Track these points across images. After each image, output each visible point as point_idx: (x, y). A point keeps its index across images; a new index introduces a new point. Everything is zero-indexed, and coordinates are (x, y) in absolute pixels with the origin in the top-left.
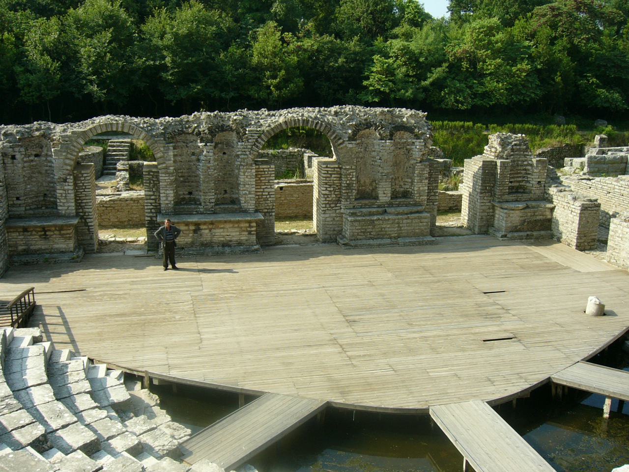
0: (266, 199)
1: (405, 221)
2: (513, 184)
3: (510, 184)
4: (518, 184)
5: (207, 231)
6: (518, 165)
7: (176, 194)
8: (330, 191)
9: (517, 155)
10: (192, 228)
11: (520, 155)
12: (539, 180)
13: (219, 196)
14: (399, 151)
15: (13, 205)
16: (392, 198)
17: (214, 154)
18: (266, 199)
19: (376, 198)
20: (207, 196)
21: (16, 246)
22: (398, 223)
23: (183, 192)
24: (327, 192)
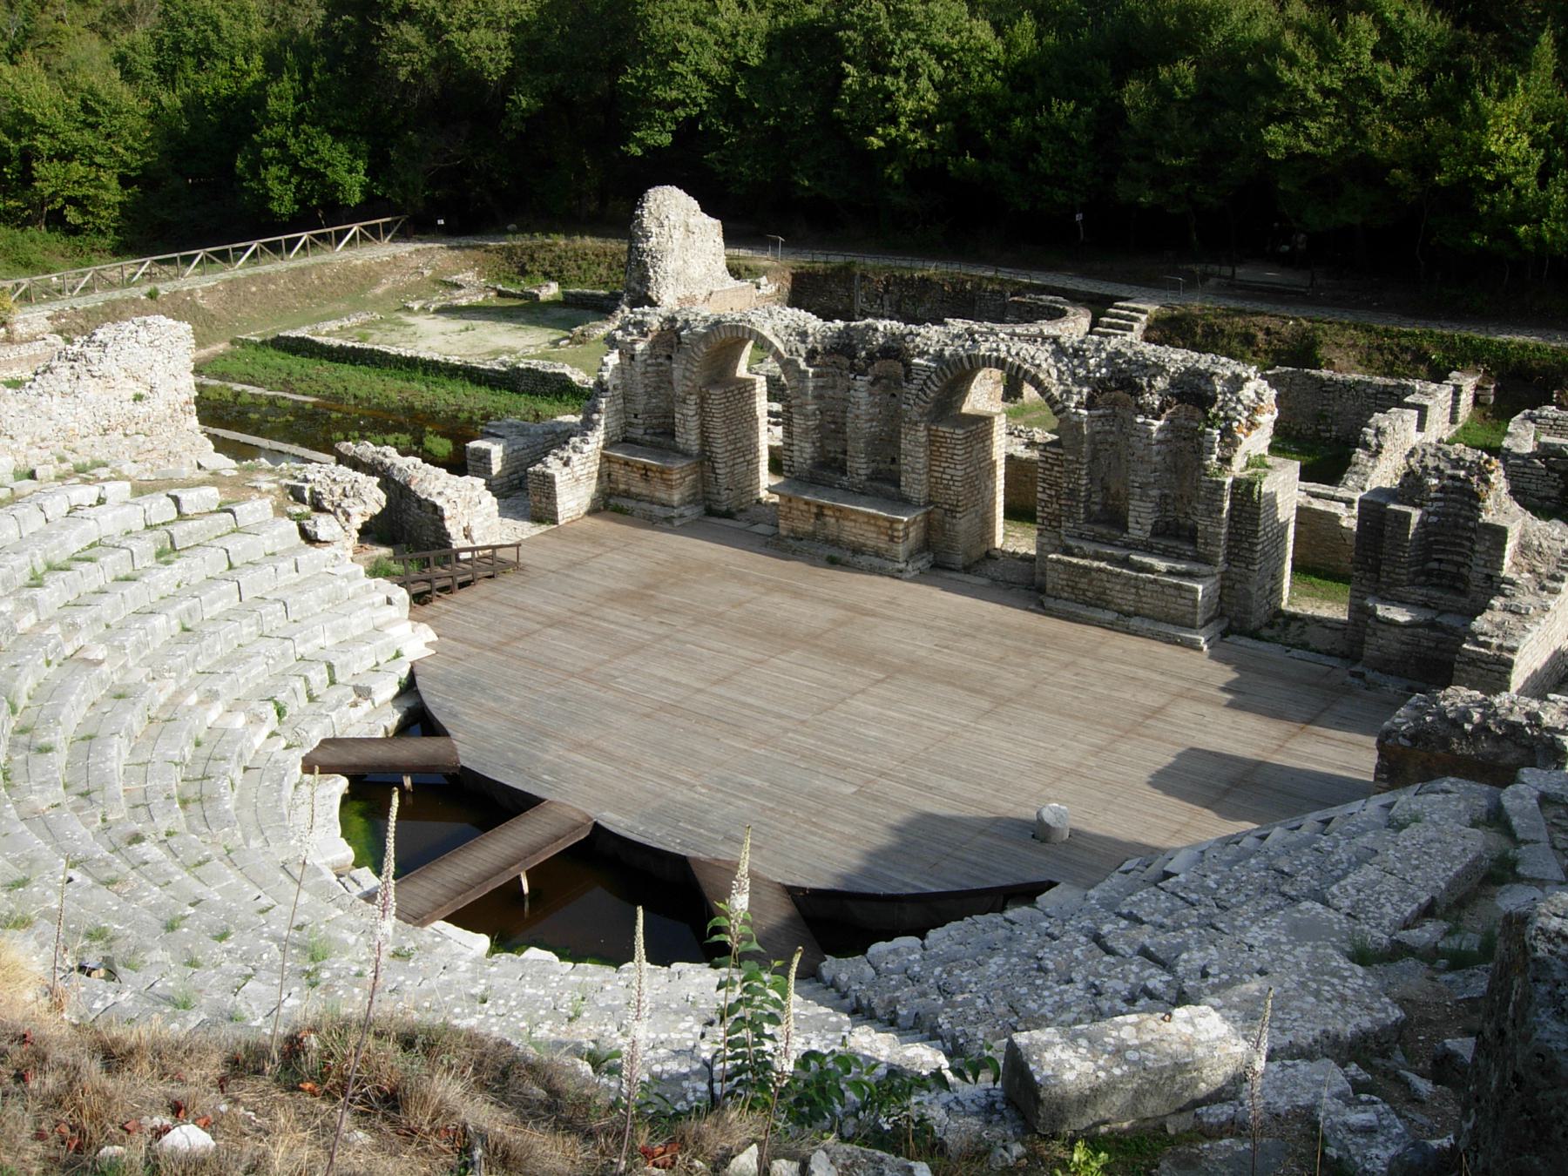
0: (947, 487)
1: (1149, 586)
2: (1444, 567)
3: (1434, 565)
4: (1453, 569)
5: (833, 520)
6: (1456, 526)
7: (821, 448)
8: (1050, 496)
9: (1455, 501)
10: (814, 510)
11: (1462, 503)
12: (1486, 571)
13: (881, 466)
14: (1183, 444)
15: (631, 424)
16: (1154, 534)
17: (871, 394)
18: (947, 487)
19: (1124, 528)
20: (860, 466)
21: (617, 482)
22: (1137, 588)
23: (832, 447)
24: (1045, 497)
